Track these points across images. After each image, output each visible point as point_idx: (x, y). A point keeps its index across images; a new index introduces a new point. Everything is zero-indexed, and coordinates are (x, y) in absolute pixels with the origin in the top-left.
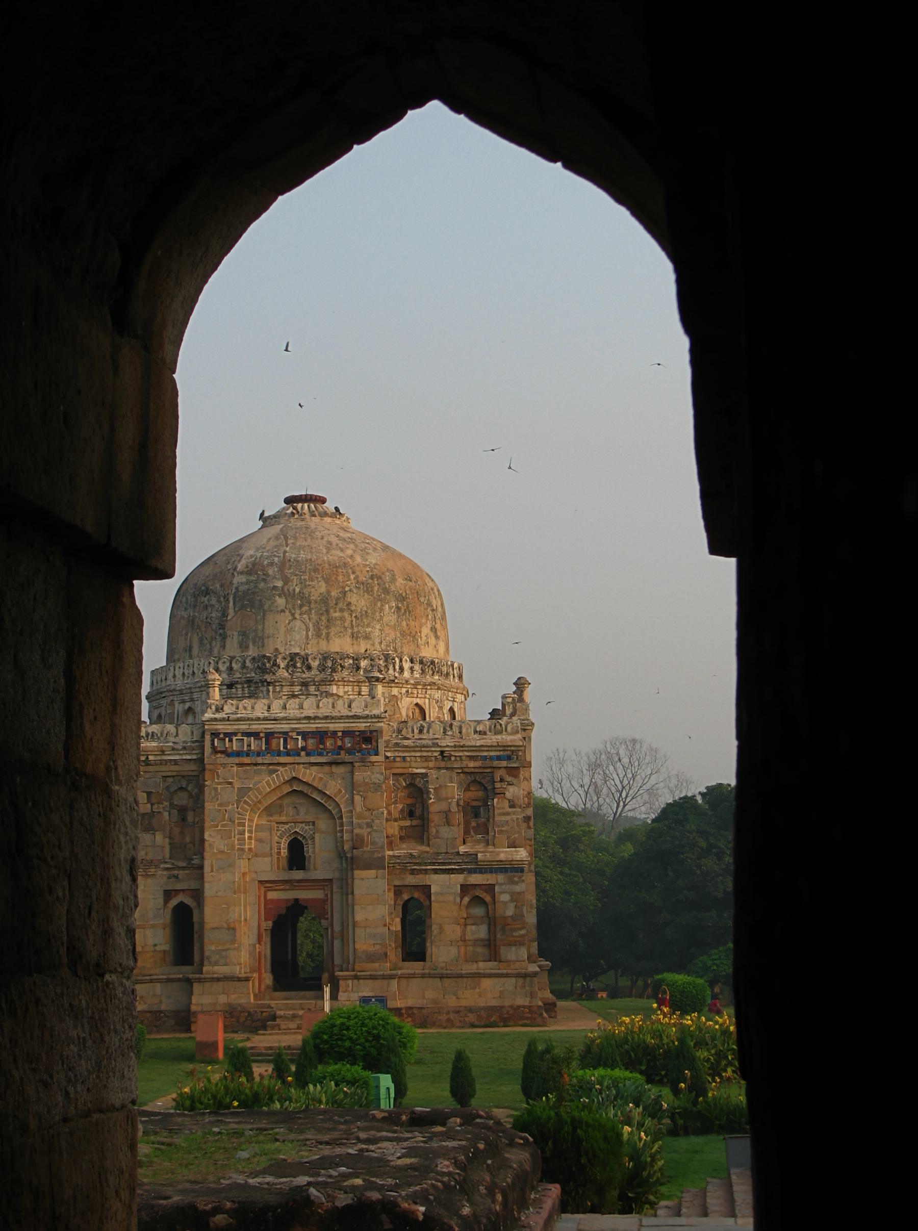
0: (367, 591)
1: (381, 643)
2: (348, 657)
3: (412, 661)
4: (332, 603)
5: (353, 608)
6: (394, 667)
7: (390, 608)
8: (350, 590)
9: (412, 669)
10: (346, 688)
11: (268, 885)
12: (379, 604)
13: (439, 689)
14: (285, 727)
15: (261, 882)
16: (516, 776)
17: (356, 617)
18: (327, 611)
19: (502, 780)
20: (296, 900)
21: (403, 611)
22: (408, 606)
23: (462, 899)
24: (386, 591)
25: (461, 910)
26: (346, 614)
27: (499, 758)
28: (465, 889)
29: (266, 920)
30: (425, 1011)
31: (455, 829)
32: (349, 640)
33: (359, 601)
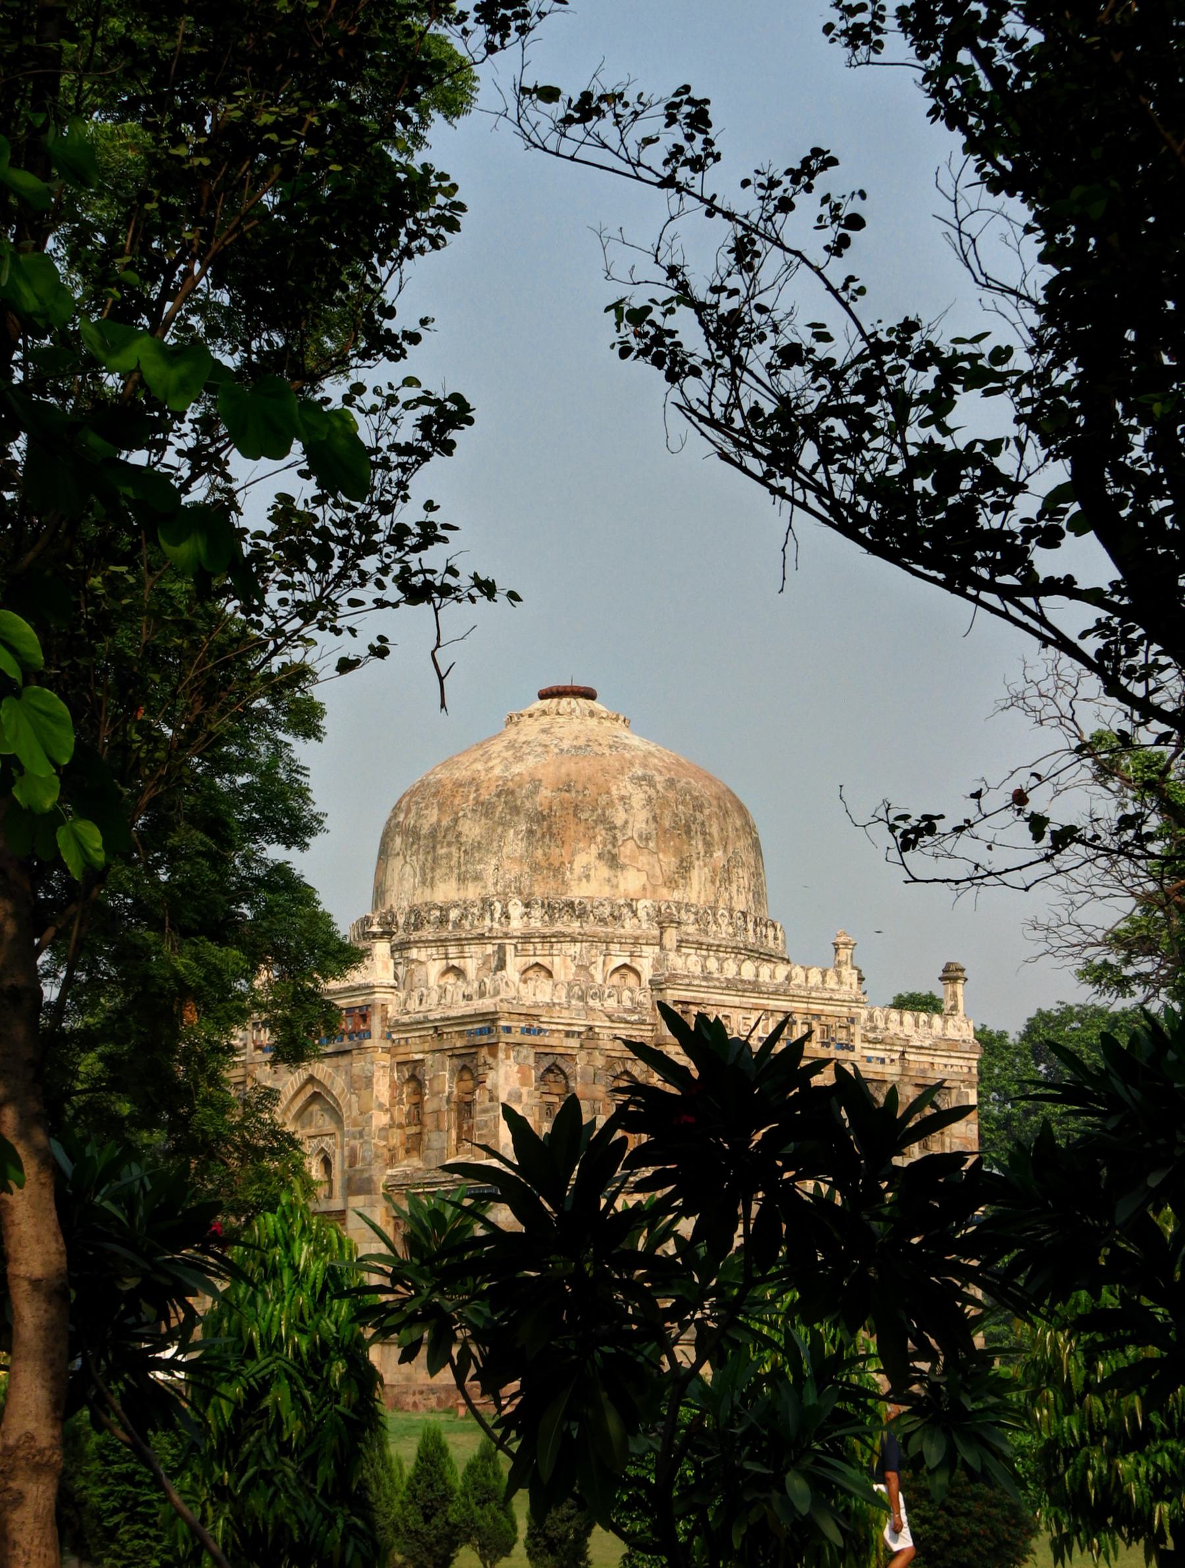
0: (486, 815)
1: (496, 884)
3: (527, 905)
5: (463, 839)
7: (517, 833)
10: (430, 951)
12: (500, 830)
13: (574, 941)
18: (434, 848)
21: (539, 835)
22: (550, 827)
24: (516, 810)
26: (454, 849)
27: (481, 1032)
30: (396, 1390)
31: (444, 1135)
32: (453, 883)
33: (472, 830)
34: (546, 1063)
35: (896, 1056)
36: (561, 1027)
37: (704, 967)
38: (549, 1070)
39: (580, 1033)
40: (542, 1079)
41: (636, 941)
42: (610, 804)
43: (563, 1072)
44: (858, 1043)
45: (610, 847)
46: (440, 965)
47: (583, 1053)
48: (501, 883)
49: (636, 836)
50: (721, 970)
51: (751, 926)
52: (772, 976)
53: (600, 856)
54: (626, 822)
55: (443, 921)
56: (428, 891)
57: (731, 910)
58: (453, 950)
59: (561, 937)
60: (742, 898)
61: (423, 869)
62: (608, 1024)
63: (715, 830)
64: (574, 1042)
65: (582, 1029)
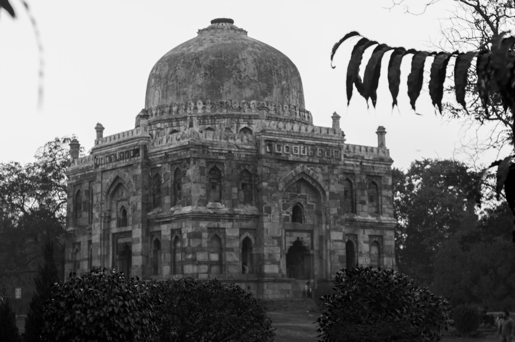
0: (188, 68)
1: (192, 96)
2: (167, 107)
3: (204, 104)
4: (169, 77)
5: (179, 78)
6: (190, 108)
7: (200, 75)
8: (179, 69)
9: (204, 108)
11: (116, 235)
12: (193, 74)
14: (114, 149)
15: (114, 234)
16: (189, 163)
17: (179, 83)
18: (167, 82)
19: (185, 167)
20: (126, 243)
21: (209, 75)
22: (214, 72)
23: (172, 237)
24: (199, 66)
25: (171, 244)
28: (173, 231)
29: (117, 254)
32: (175, 97)
34: (211, 166)
35: (358, 164)
36: (217, 151)
37: (277, 126)
38: (212, 169)
39: (225, 154)
40: (210, 172)
41: (250, 117)
42: (238, 62)
43: (219, 170)
44: (343, 158)
45: (238, 79)
46: (169, 130)
47: (228, 162)
48: (194, 95)
49: (249, 75)
50: (285, 127)
51: (298, 112)
52: (306, 130)
53: (234, 83)
54: (245, 69)
55: (170, 112)
56: (165, 101)
57: (289, 105)
58: (174, 123)
59: (219, 116)
60: (294, 101)
61: (163, 91)
62: (237, 150)
63: (282, 72)
64: (222, 157)
65: (227, 152)
